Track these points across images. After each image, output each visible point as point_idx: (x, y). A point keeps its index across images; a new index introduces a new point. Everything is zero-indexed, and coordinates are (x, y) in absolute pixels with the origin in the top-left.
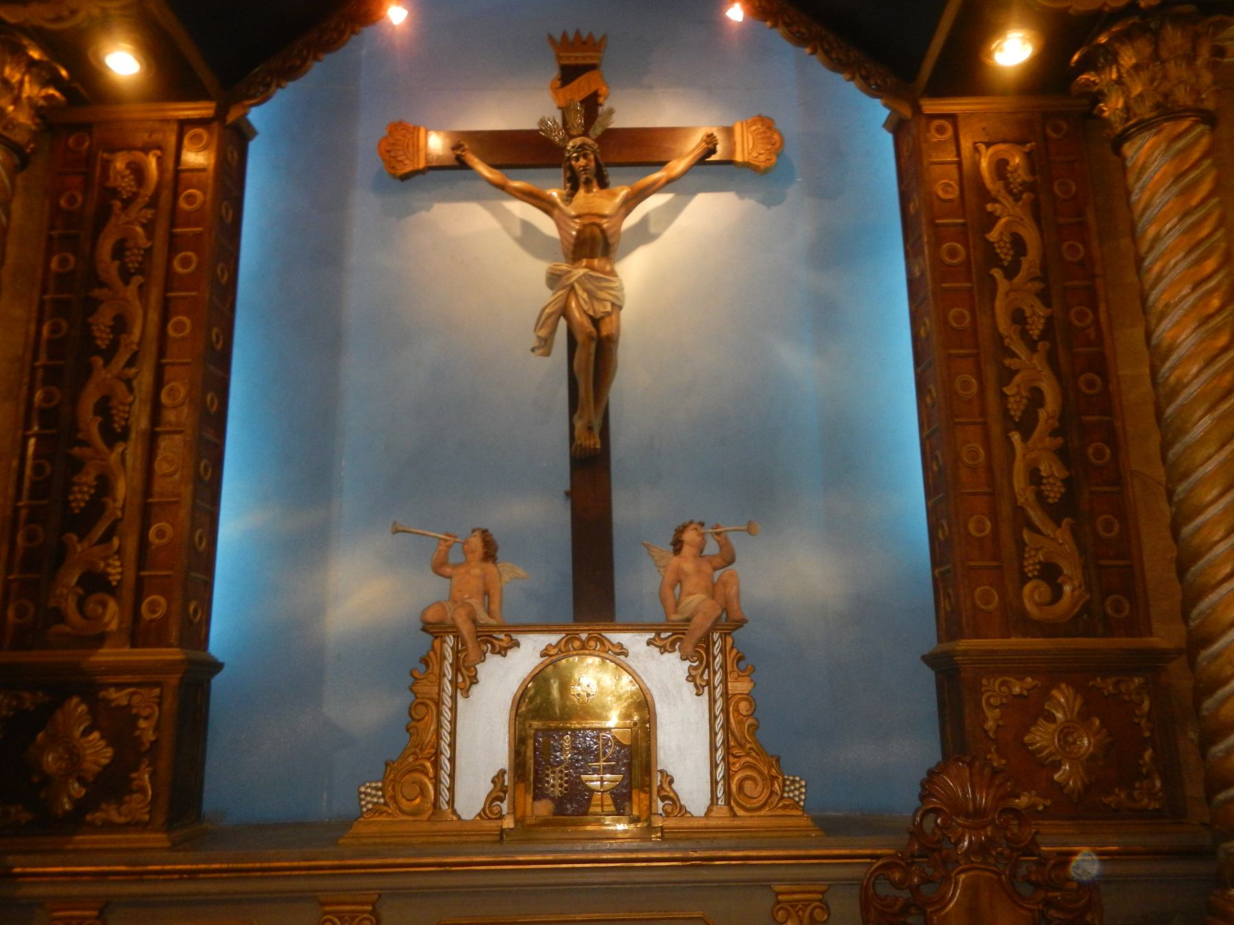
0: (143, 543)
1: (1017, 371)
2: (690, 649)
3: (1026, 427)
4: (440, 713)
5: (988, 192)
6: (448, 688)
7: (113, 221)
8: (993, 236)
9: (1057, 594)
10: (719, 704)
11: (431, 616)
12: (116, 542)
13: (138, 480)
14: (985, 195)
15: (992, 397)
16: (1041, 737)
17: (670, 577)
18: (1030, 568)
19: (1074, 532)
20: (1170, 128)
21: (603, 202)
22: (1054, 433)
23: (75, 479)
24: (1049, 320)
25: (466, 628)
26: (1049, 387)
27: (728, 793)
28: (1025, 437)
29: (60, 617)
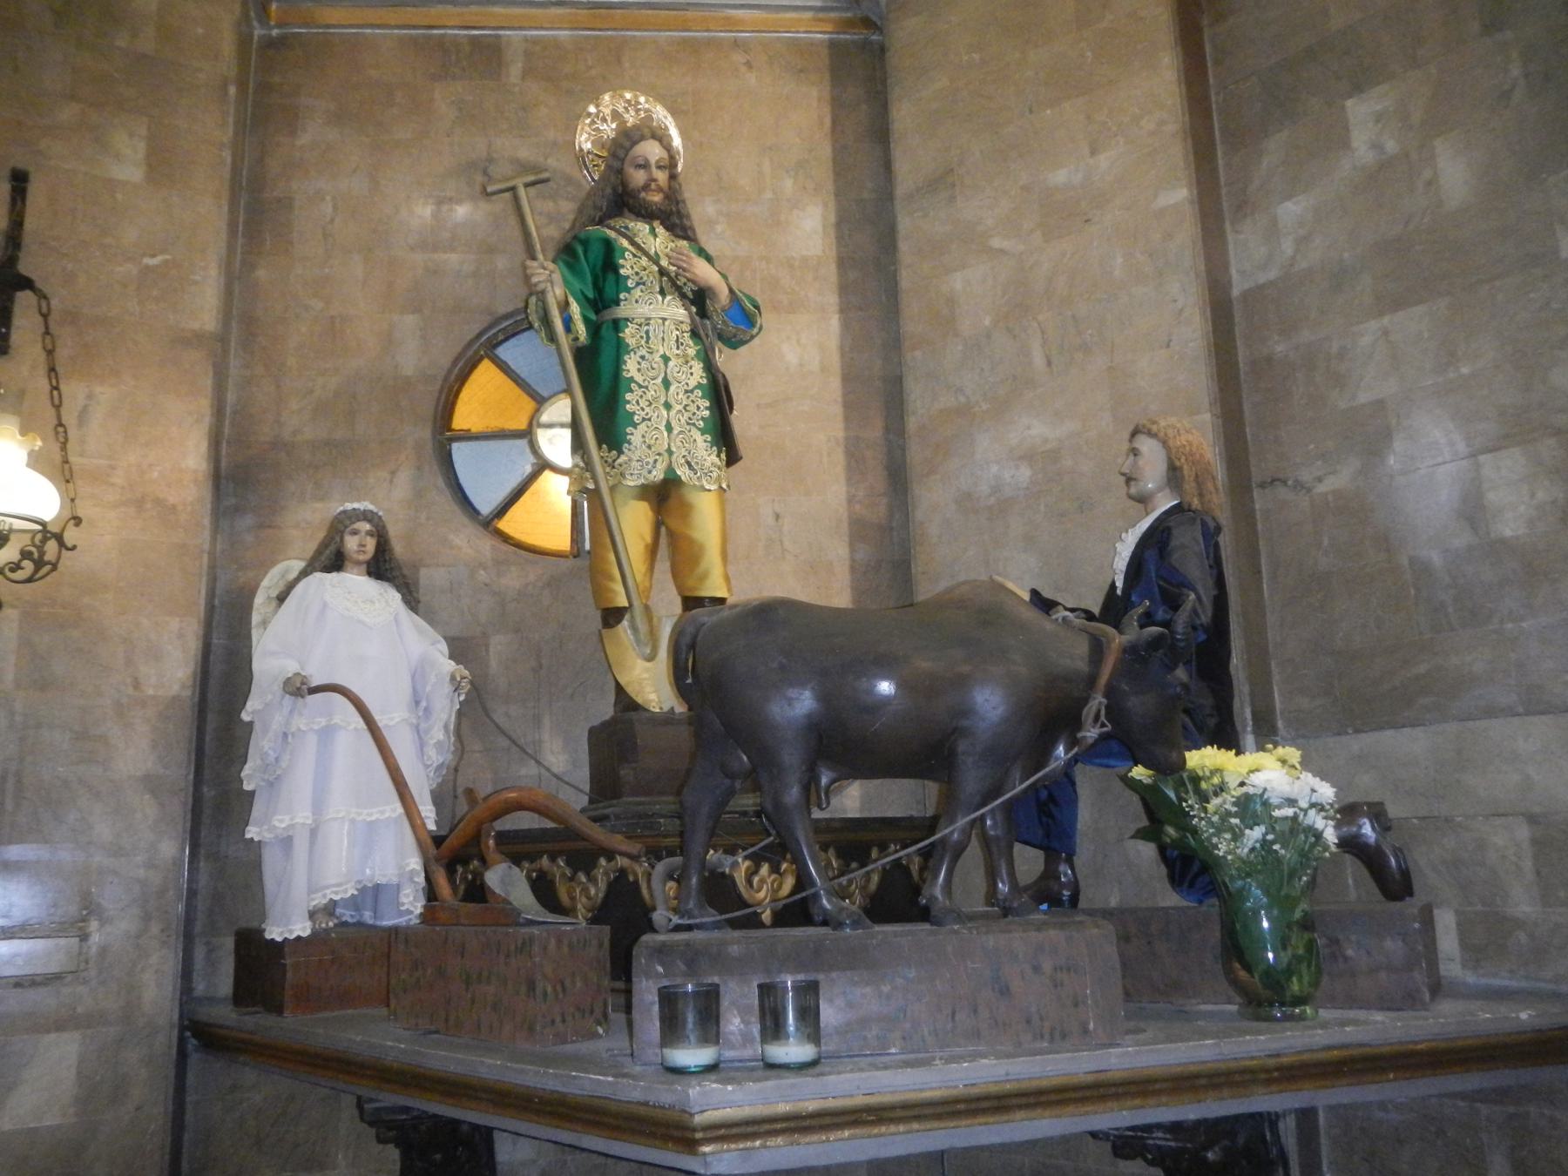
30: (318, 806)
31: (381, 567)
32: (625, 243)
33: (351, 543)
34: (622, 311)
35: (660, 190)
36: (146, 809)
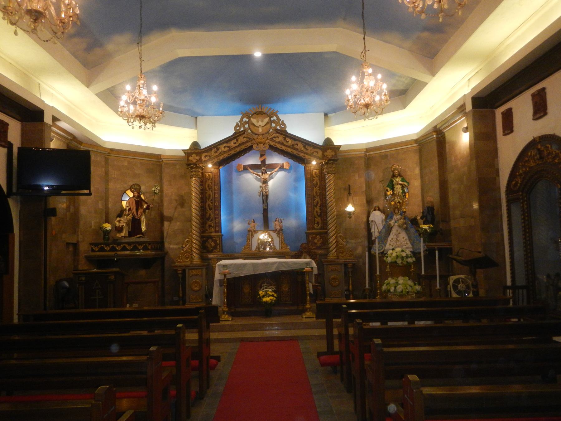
0: (215, 221)
3: (316, 206)
4: (250, 240)
6: (251, 237)
7: (207, 182)
8: (314, 182)
9: (318, 226)
10: (280, 238)
11: (249, 229)
13: (214, 214)
14: (313, 177)
16: (316, 241)
17: (275, 224)
18: (316, 222)
19: (321, 218)
20: (329, 175)
21: (266, 176)
22: (319, 207)
24: (320, 193)
25: (253, 231)
26: (319, 201)
28: (316, 207)
29: (207, 230)
30: (375, 230)
31: (379, 210)
32: (394, 180)
33: (376, 208)
34: (395, 186)
36: (364, 230)
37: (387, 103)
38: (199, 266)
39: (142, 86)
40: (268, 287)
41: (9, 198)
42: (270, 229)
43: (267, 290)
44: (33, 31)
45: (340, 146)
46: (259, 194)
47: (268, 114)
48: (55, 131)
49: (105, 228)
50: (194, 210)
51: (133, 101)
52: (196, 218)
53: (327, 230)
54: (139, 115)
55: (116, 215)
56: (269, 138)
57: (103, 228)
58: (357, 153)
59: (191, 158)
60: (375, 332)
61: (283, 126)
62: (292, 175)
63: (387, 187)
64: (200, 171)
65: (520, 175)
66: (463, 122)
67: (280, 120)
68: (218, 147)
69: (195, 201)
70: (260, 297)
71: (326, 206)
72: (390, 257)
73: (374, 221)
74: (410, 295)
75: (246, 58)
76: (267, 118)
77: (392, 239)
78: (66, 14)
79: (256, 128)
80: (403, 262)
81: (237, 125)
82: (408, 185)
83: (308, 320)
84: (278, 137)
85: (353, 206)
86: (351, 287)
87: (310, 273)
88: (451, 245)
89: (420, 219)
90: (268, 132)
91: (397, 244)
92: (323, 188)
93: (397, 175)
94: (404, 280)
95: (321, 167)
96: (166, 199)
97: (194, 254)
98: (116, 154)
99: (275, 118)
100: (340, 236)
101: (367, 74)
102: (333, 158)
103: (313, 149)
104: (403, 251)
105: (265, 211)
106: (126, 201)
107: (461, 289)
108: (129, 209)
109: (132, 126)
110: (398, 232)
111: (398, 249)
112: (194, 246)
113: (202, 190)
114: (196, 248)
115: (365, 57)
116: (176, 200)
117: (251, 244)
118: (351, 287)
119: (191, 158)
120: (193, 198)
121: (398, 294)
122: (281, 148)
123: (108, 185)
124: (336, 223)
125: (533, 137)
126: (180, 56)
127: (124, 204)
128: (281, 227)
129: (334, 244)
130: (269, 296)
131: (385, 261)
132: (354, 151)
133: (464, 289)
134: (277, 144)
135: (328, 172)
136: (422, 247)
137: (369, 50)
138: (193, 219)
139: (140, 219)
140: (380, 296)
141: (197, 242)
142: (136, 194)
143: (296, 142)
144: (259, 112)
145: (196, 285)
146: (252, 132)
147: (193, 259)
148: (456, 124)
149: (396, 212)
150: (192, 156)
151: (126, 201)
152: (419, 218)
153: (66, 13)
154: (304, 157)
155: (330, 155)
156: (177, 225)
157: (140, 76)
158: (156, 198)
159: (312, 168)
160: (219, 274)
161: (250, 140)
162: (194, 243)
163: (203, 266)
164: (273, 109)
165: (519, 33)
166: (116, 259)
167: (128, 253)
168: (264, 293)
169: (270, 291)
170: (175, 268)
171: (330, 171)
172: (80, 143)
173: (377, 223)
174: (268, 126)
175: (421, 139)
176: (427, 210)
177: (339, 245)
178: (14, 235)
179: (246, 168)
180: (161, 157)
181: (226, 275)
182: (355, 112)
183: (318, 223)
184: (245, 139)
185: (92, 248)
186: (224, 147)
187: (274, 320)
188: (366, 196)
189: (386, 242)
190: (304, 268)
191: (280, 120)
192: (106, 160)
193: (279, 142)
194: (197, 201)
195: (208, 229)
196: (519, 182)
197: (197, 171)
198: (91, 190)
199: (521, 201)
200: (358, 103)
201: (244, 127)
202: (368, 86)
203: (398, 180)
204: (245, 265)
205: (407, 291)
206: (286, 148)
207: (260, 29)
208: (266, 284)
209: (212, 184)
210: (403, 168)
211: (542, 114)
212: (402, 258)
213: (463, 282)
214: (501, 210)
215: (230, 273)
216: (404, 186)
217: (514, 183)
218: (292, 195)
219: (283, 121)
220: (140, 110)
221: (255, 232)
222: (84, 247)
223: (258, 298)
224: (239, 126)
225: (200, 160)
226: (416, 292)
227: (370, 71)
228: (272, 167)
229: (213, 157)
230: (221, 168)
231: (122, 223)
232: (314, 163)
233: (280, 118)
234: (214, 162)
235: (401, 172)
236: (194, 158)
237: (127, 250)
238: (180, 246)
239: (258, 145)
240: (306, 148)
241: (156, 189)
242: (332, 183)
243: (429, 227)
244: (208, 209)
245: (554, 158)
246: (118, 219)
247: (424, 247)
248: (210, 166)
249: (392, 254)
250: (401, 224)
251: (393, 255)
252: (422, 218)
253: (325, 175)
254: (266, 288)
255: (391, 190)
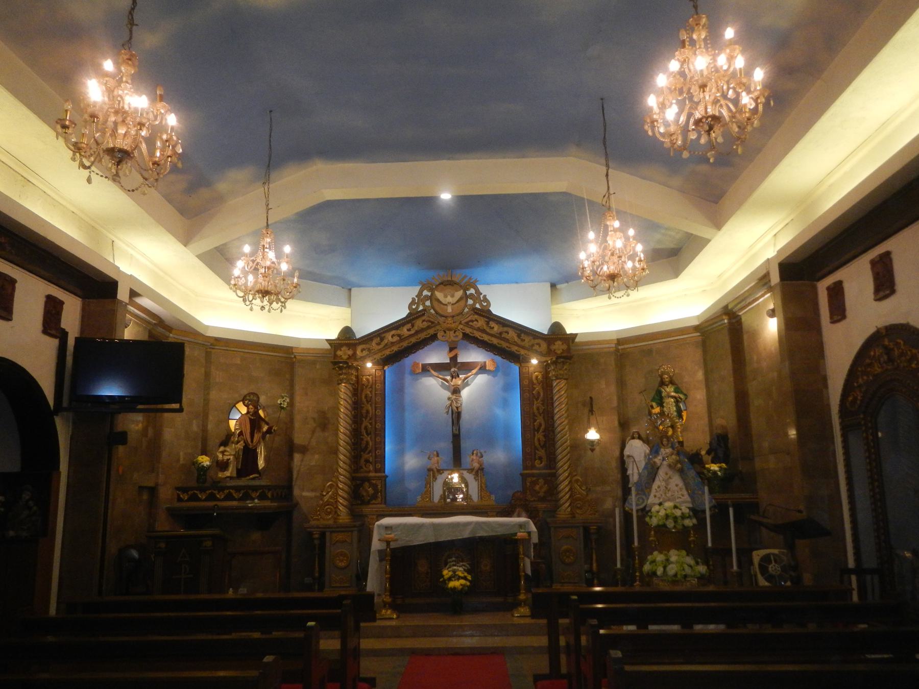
1: (536, 420)
2: (474, 473)
3: (538, 430)
4: (430, 485)
5: (533, 383)
6: (432, 480)
9: (541, 463)
11: (429, 467)
12: (370, 454)
14: (533, 384)
15: (532, 424)
16: (537, 488)
17: (471, 459)
19: (546, 451)
20: (558, 381)
21: (459, 382)
22: (543, 432)
23: (363, 442)
24: (544, 409)
25: (435, 470)
26: (543, 422)
27: (481, 498)
28: (538, 433)
31: (640, 438)
33: (635, 436)
34: (664, 401)
35: (667, 381)
37: (644, 273)
38: (347, 527)
39: (268, 247)
40: (458, 563)
41: (57, 415)
42: (463, 466)
43: (455, 569)
44: (114, 177)
45: (576, 335)
46: (447, 410)
47: (462, 284)
48: (131, 311)
49: (200, 463)
50: (341, 436)
51: (253, 268)
52: (345, 449)
53: (554, 471)
54: (261, 291)
55: (218, 441)
56: (463, 322)
57: (197, 463)
58: (601, 346)
59: (339, 353)
60: (614, 641)
61: (485, 304)
62: (500, 380)
63: (653, 400)
64: (352, 374)
65: (860, 386)
66: (768, 301)
67: (481, 294)
68: (383, 335)
69: (344, 420)
70: (444, 581)
71: (553, 432)
72: (656, 516)
73: (632, 457)
74: (689, 580)
75: (429, 202)
76: (460, 290)
77: (659, 487)
78: (162, 153)
79: (442, 306)
80: (677, 526)
81: (413, 302)
82: (686, 399)
83: (522, 621)
84: (478, 322)
85: (596, 432)
86: (595, 565)
87: (526, 541)
88: (757, 498)
89: (706, 454)
90: (461, 313)
91: (668, 495)
92: (549, 401)
93: (667, 383)
94: (679, 556)
95: (545, 368)
96: (298, 418)
97: (339, 507)
98: (222, 346)
99: (472, 291)
100: (577, 481)
101: (612, 229)
102: (564, 355)
103: (532, 341)
104: (675, 507)
105: (456, 438)
106: (236, 421)
107: (774, 573)
108: (239, 433)
109: (250, 306)
110: (668, 476)
111: (669, 504)
112: (340, 493)
113: (355, 403)
114: (343, 498)
115: (609, 203)
116: (314, 419)
117: (432, 491)
118: (595, 565)
119: (339, 353)
120: (341, 416)
121: (670, 579)
122: (482, 337)
123: (208, 394)
124: (569, 459)
125: (877, 327)
126: (329, 199)
127: (232, 424)
128: (481, 464)
129: (566, 493)
130: (459, 578)
131: (647, 524)
132: (599, 342)
133: (779, 573)
134: (475, 332)
135: (556, 377)
136: (707, 501)
137: (614, 193)
138: (340, 450)
139: (256, 449)
140: (639, 582)
141: (346, 488)
142: (252, 409)
143: (505, 329)
144: (448, 281)
145: (341, 558)
146: (437, 312)
147: (338, 515)
148: (758, 304)
149: (664, 443)
150: (342, 349)
151: (236, 421)
152: (703, 453)
153: (162, 150)
154: (519, 352)
155: (559, 350)
156: (314, 459)
157: (265, 232)
158: (283, 415)
159: (531, 369)
160: (379, 540)
161: (433, 325)
162: (341, 489)
163: (355, 526)
164: (468, 278)
165: (847, 167)
166: (215, 514)
167: (235, 503)
168: (450, 573)
169: (461, 571)
170: (309, 530)
171: (560, 375)
172: (169, 329)
173: (636, 460)
174: (462, 303)
175: (707, 324)
176: (716, 439)
177: (575, 495)
178: (60, 473)
179: (426, 369)
180: (294, 351)
181: (389, 544)
182: (595, 287)
183: (540, 458)
184: (425, 323)
185: (178, 495)
186: (392, 336)
187: (468, 620)
188: (619, 417)
189: (648, 493)
190: (516, 533)
191: (481, 294)
192: (208, 355)
193: (479, 328)
194: (347, 421)
195: (364, 467)
196: (859, 398)
197: (349, 373)
198: (183, 405)
199: (864, 428)
200: (598, 272)
201: (424, 304)
202: (613, 247)
203: (670, 389)
204: (421, 526)
205: (684, 574)
206: (489, 337)
207: (449, 159)
208: (454, 559)
209: (372, 394)
210: (677, 371)
211: (888, 292)
212: (675, 519)
213: (776, 562)
214: (833, 443)
215: (396, 540)
216: (680, 400)
217: (850, 399)
218: (499, 412)
219: (485, 296)
220: (263, 283)
221: (440, 471)
222: (166, 494)
223: (441, 582)
224: (416, 303)
225: (353, 356)
226: (699, 575)
227: (617, 224)
228: (467, 367)
229: (373, 352)
230: (386, 368)
231: (227, 455)
232: (534, 361)
233: (481, 292)
234: (375, 359)
235: (674, 378)
236: (344, 353)
237: (233, 499)
238: (318, 494)
239: (445, 332)
240: (521, 338)
241: (284, 401)
242: (564, 394)
243: (720, 467)
244: (365, 434)
245: (910, 361)
246: (222, 449)
247: (710, 502)
248: (369, 365)
249: (658, 512)
250: (673, 462)
251: (660, 514)
252: (708, 453)
253: (552, 380)
254: (455, 565)
255: (658, 407)
